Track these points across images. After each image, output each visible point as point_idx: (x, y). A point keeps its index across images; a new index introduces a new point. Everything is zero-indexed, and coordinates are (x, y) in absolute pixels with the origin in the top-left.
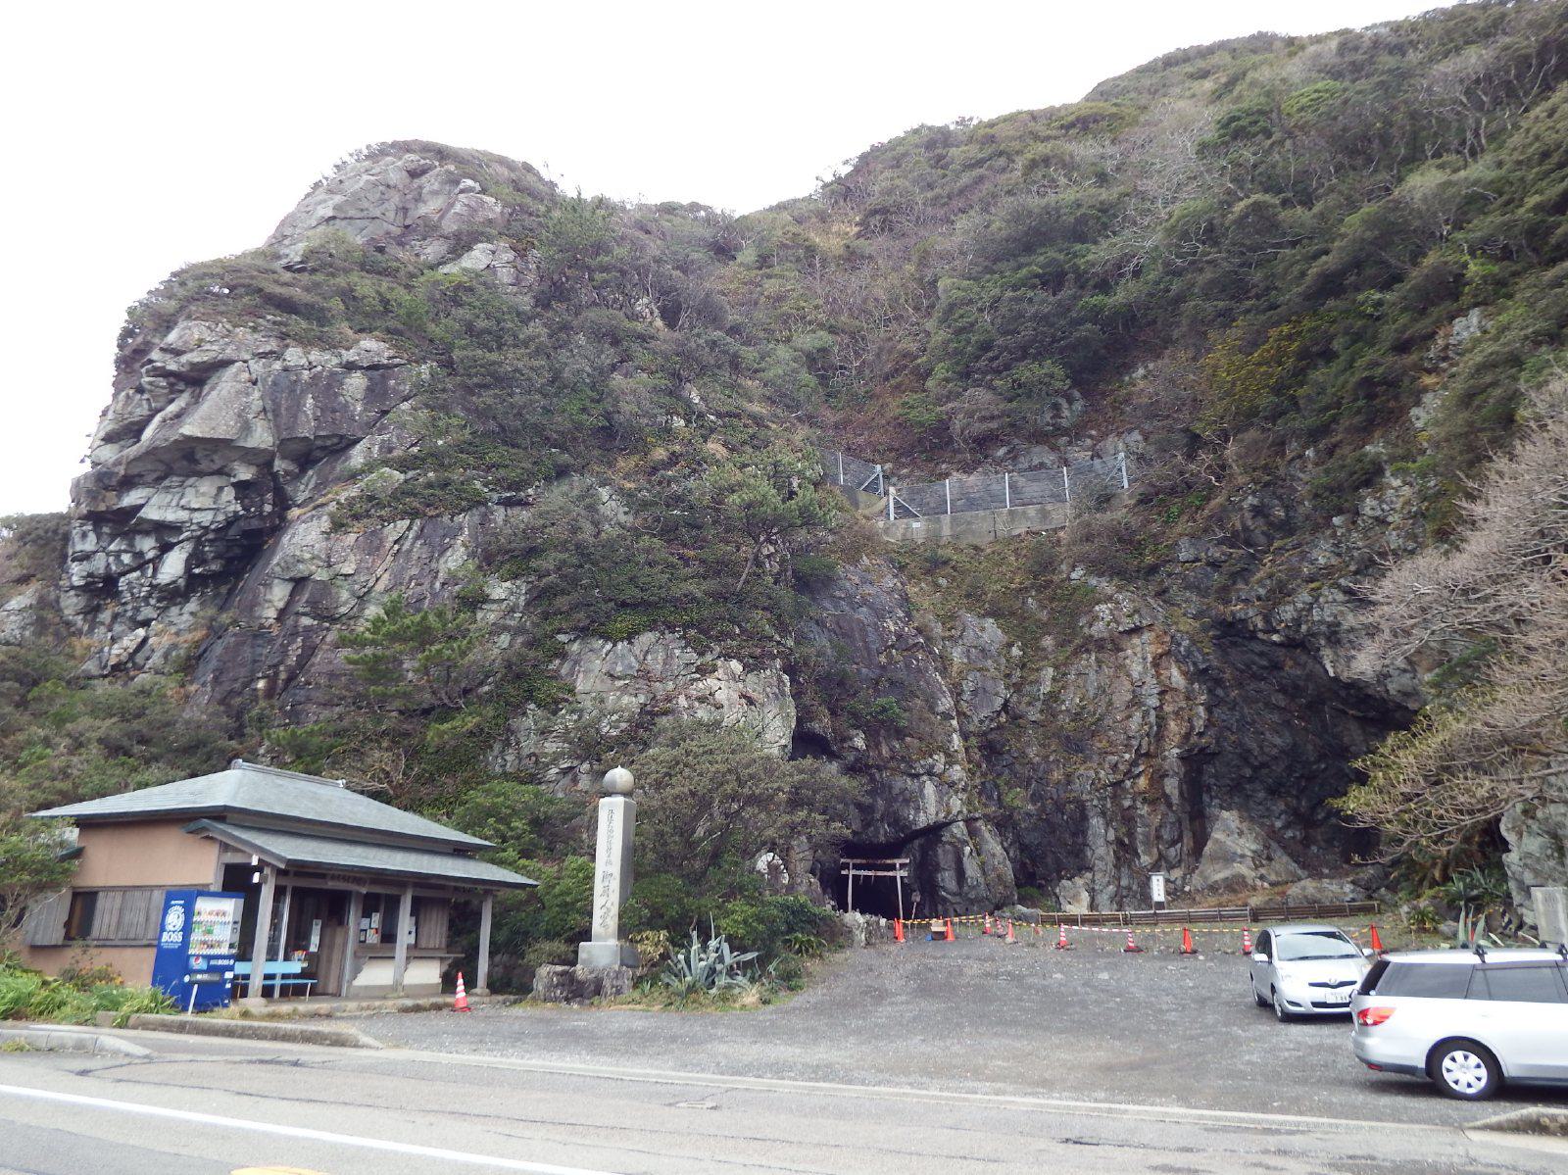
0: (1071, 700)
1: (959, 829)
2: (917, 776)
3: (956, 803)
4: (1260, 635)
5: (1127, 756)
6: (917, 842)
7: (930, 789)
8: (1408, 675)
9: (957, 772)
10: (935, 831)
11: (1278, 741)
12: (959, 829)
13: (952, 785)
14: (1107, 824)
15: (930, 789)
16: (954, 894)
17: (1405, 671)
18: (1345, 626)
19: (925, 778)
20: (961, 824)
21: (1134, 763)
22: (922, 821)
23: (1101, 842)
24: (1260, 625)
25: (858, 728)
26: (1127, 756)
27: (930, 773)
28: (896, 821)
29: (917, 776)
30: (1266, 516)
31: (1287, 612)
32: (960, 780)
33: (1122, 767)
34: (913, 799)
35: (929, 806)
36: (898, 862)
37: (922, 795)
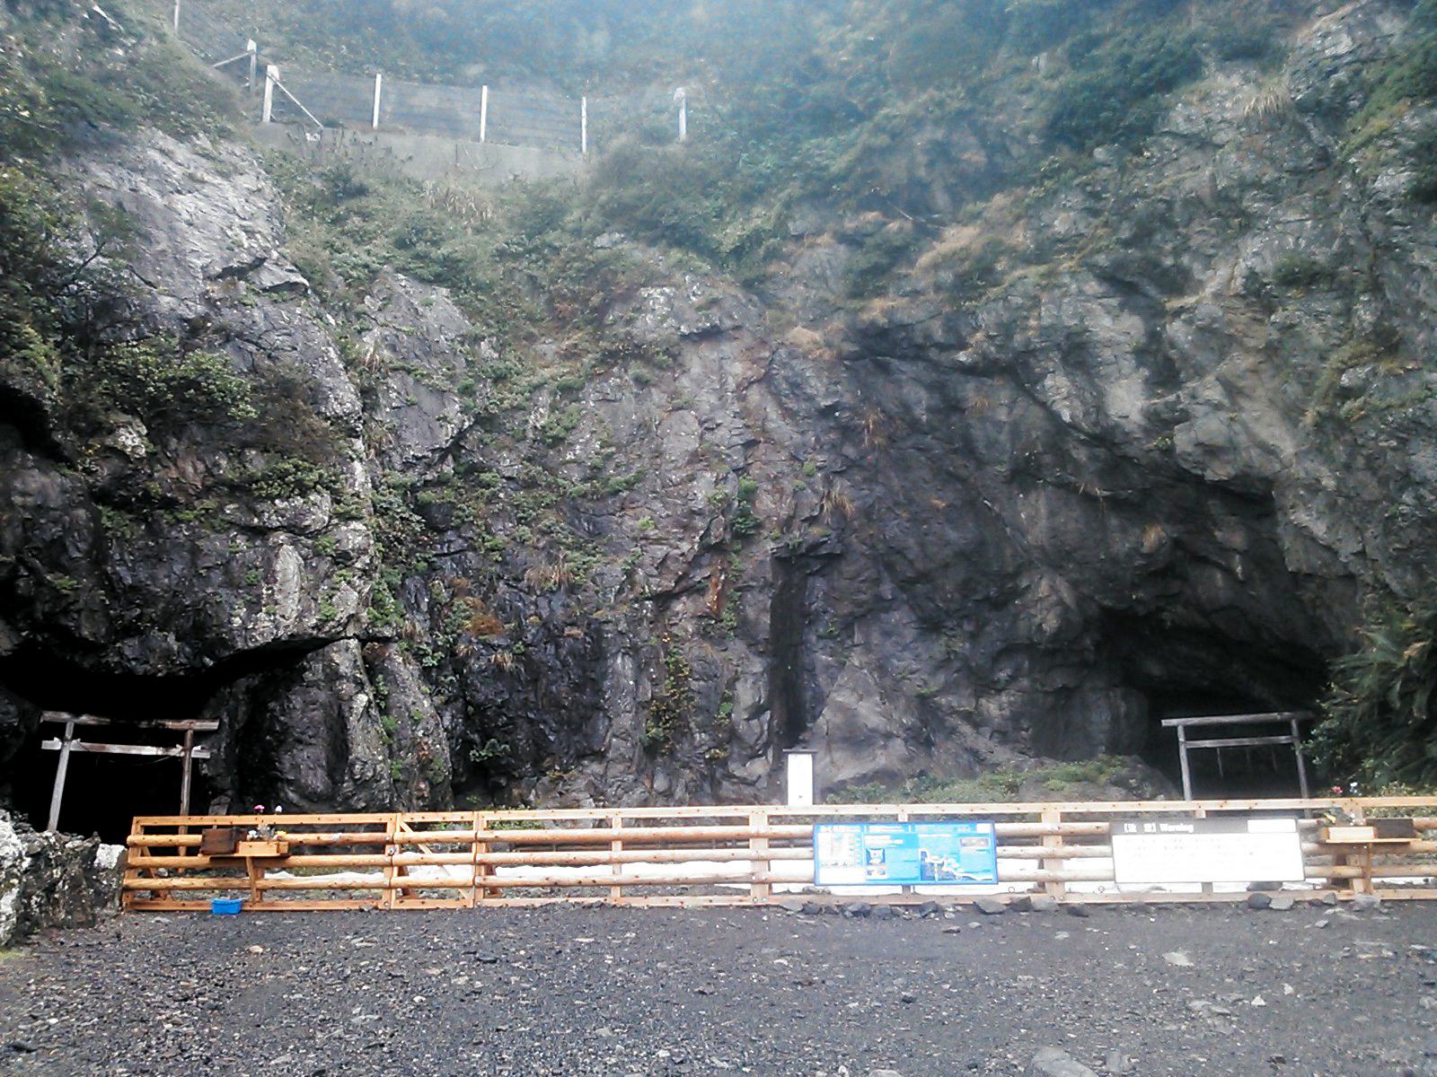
0: (586, 446)
1: (345, 656)
2: (261, 532)
3: (348, 600)
5: (685, 547)
6: (243, 683)
7: (289, 562)
8: (1224, 415)
10: (288, 658)
11: (952, 535)
12: (345, 656)
13: (343, 559)
14: (640, 669)
15: (289, 562)
19: (282, 537)
20: (353, 643)
21: (695, 563)
22: (264, 630)
23: (625, 703)
26: (685, 547)
27: (295, 530)
28: (200, 628)
30: (950, 160)
34: (253, 586)
35: (286, 602)
37: (270, 576)
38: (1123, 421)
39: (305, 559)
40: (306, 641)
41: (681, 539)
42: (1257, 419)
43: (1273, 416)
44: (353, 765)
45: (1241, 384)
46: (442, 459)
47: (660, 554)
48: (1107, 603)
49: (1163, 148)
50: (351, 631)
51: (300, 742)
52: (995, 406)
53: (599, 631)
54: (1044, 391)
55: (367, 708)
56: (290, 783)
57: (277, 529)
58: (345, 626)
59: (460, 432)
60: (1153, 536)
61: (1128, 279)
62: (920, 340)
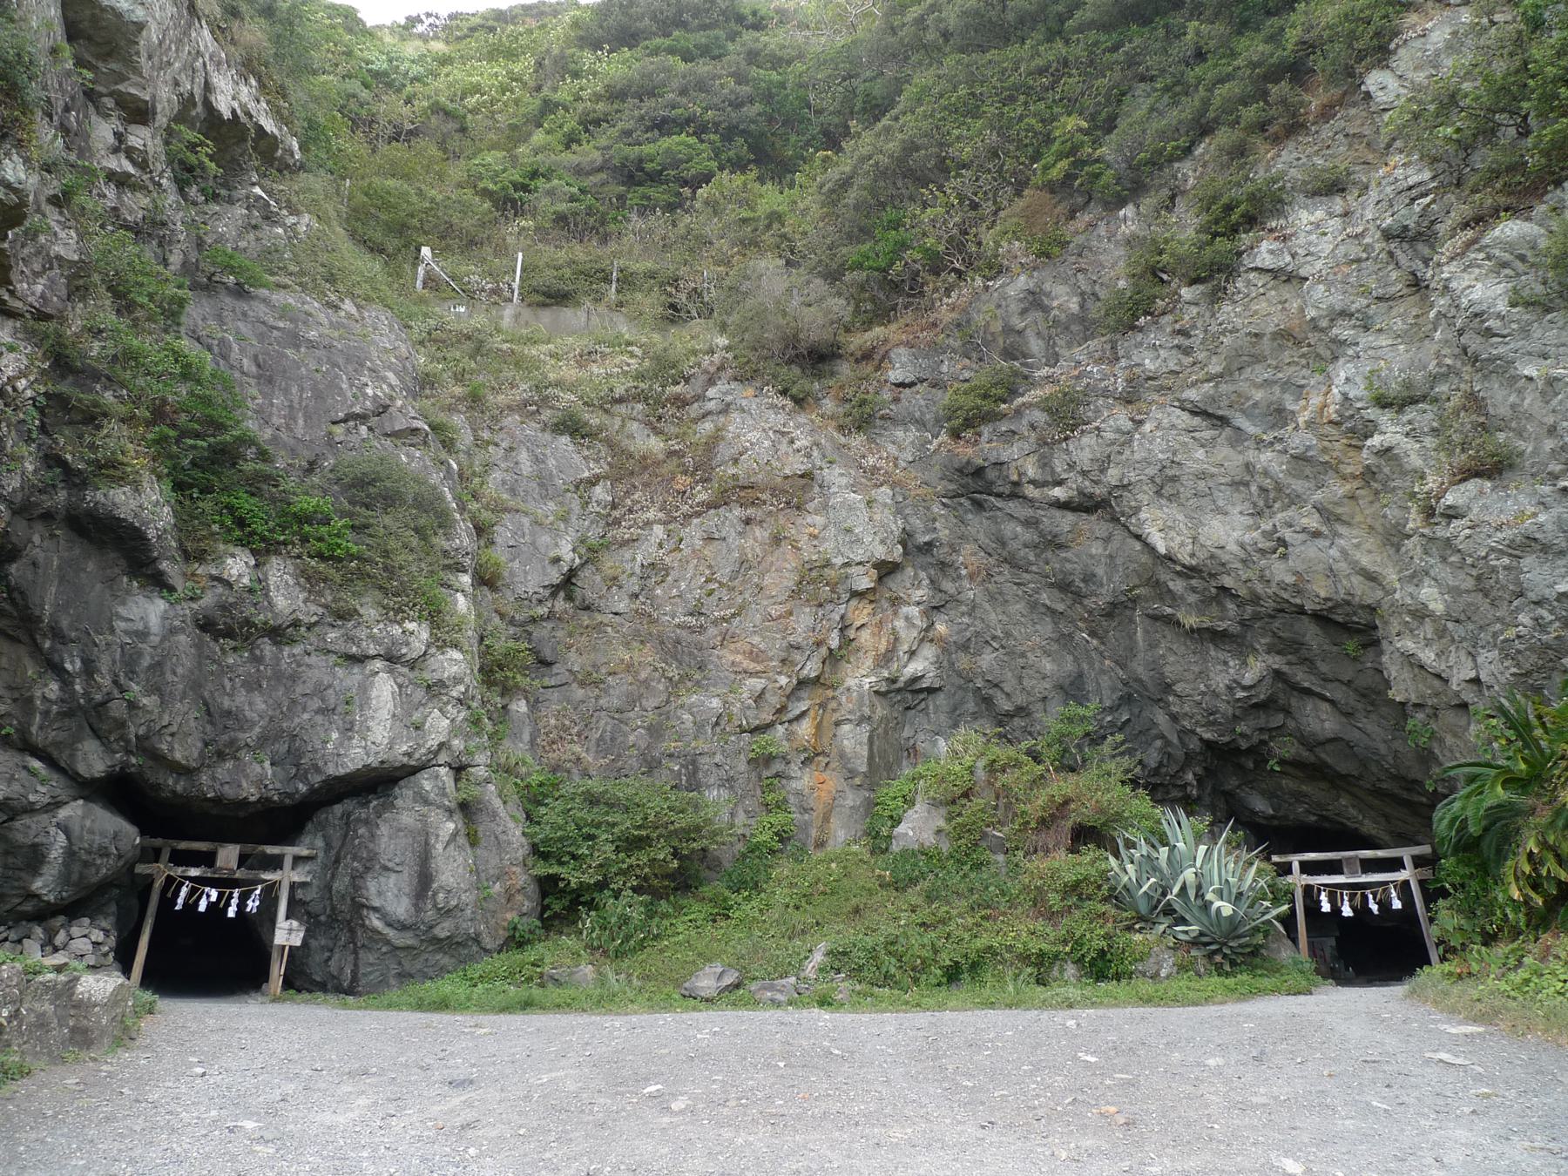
0: (688, 583)
2: (359, 660)
3: (439, 724)
4: (1030, 491)
6: (338, 809)
7: (384, 689)
9: (454, 664)
10: (379, 783)
11: (1048, 666)
13: (435, 689)
15: (384, 689)
16: (403, 927)
17: (1316, 534)
18: (1191, 467)
19: (378, 664)
22: (355, 757)
24: (1031, 471)
25: (240, 543)
26: (783, 680)
28: (293, 757)
29: (359, 660)
30: (1046, 309)
31: (1084, 449)
32: (457, 680)
33: (774, 700)
34: (346, 712)
35: (378, 727)
36: (290, 851)
37: (365, 703)
38: (1219, 552)
39: (400, 686)
40: (396, 769)
41: (780, 673)
42: (1357, 546)
43: (1371, 542)
44: (435, 894)
45: (1339, 510)
46: (554, 595)
47: (759, 687)
48: (1207, 736)
49: (1248, 283)
50: (443, 758)
51: (386, 869)
52: (1091, 544)
53: (694, 762)
54: (1141, 523)
55: (454, 835)
56: (375, 909)
57: (373, 657)
58: (437, 753)
59: (571, 570)
60: (1255, 669)
61: (1220, 413)
62: (1015, 478)
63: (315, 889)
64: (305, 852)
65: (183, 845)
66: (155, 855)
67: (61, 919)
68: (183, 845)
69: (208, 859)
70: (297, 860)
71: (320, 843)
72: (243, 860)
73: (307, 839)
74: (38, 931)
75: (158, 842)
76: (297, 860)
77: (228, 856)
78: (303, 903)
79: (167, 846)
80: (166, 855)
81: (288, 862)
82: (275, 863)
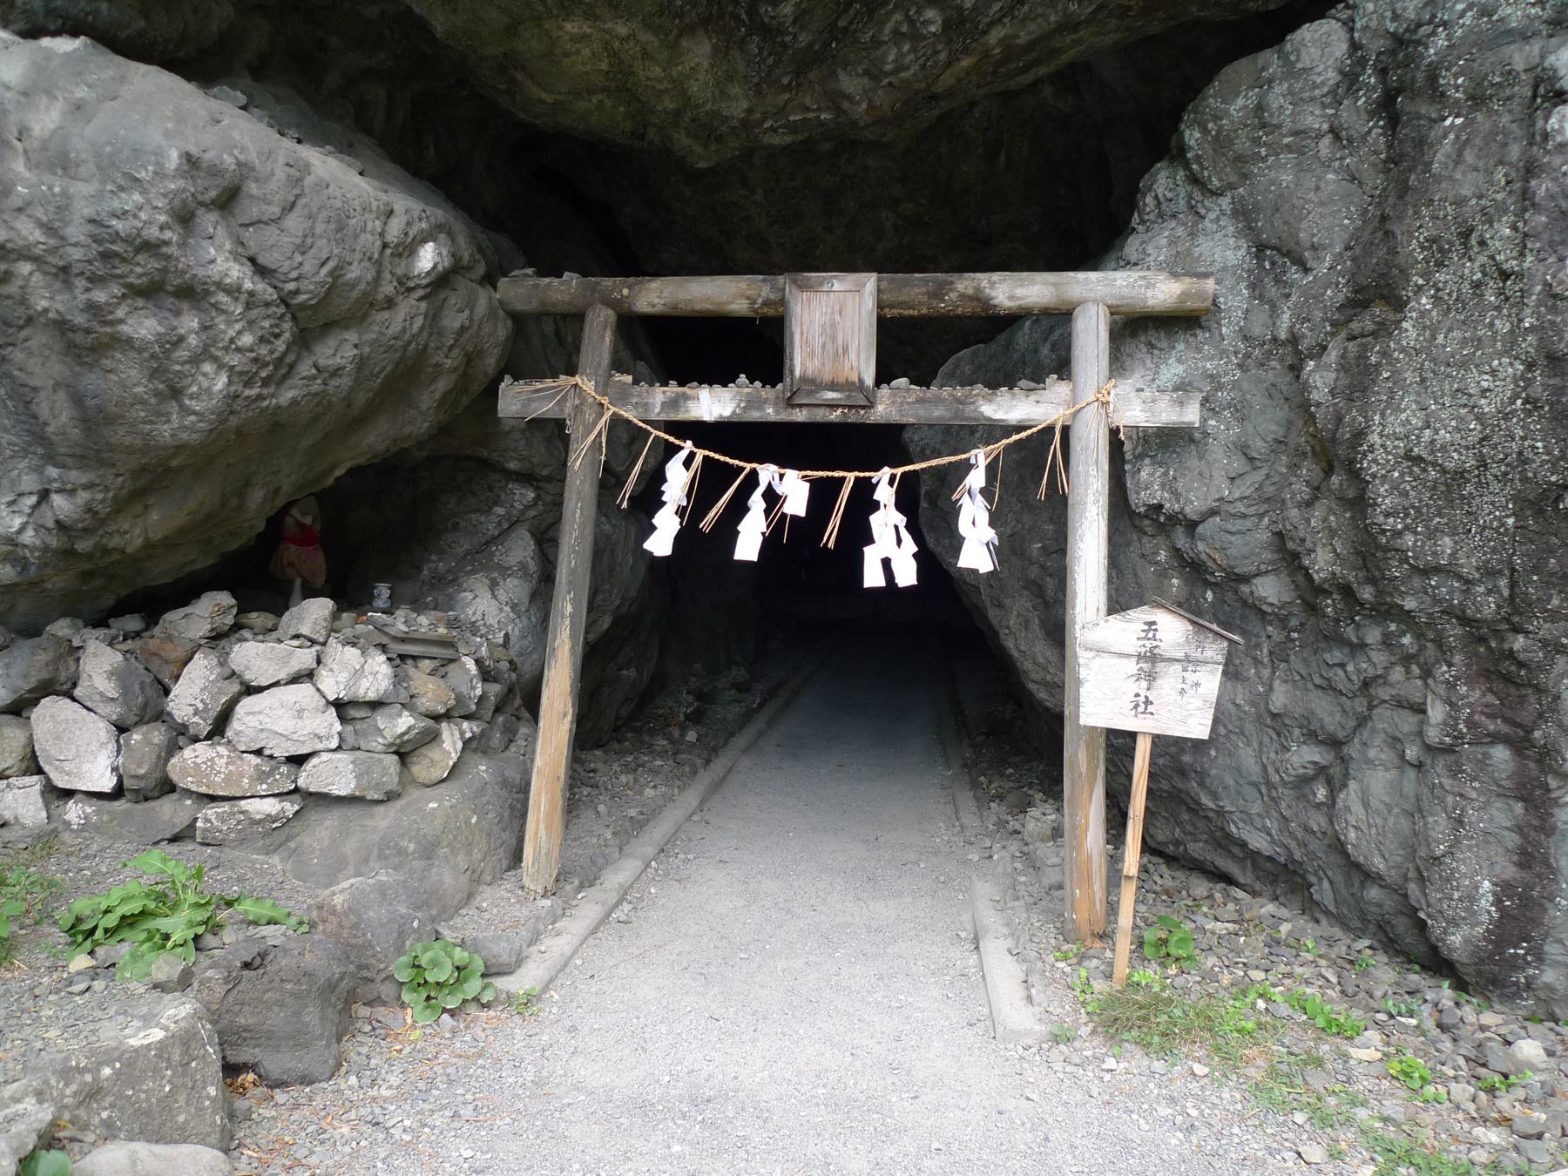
36: (1094, 294)
63: (1221, 461)
64: (1163, 292)
65: (657, 295)
66: (545, 346)
67: (213, 607)
68: (657, 295)
69: (754, 348)
70: (1136, 330)
71: (1224, 249)
72: (907, 347)
73: (1152, 239)
74: (100, 665)
75: (565, 288)
76: (1136, 330)
77: (834, 324)
78: (1163, 522)
79: (603, 302)
80: (599, 340)
81: (1091, 338)
82: (1037, 349)
